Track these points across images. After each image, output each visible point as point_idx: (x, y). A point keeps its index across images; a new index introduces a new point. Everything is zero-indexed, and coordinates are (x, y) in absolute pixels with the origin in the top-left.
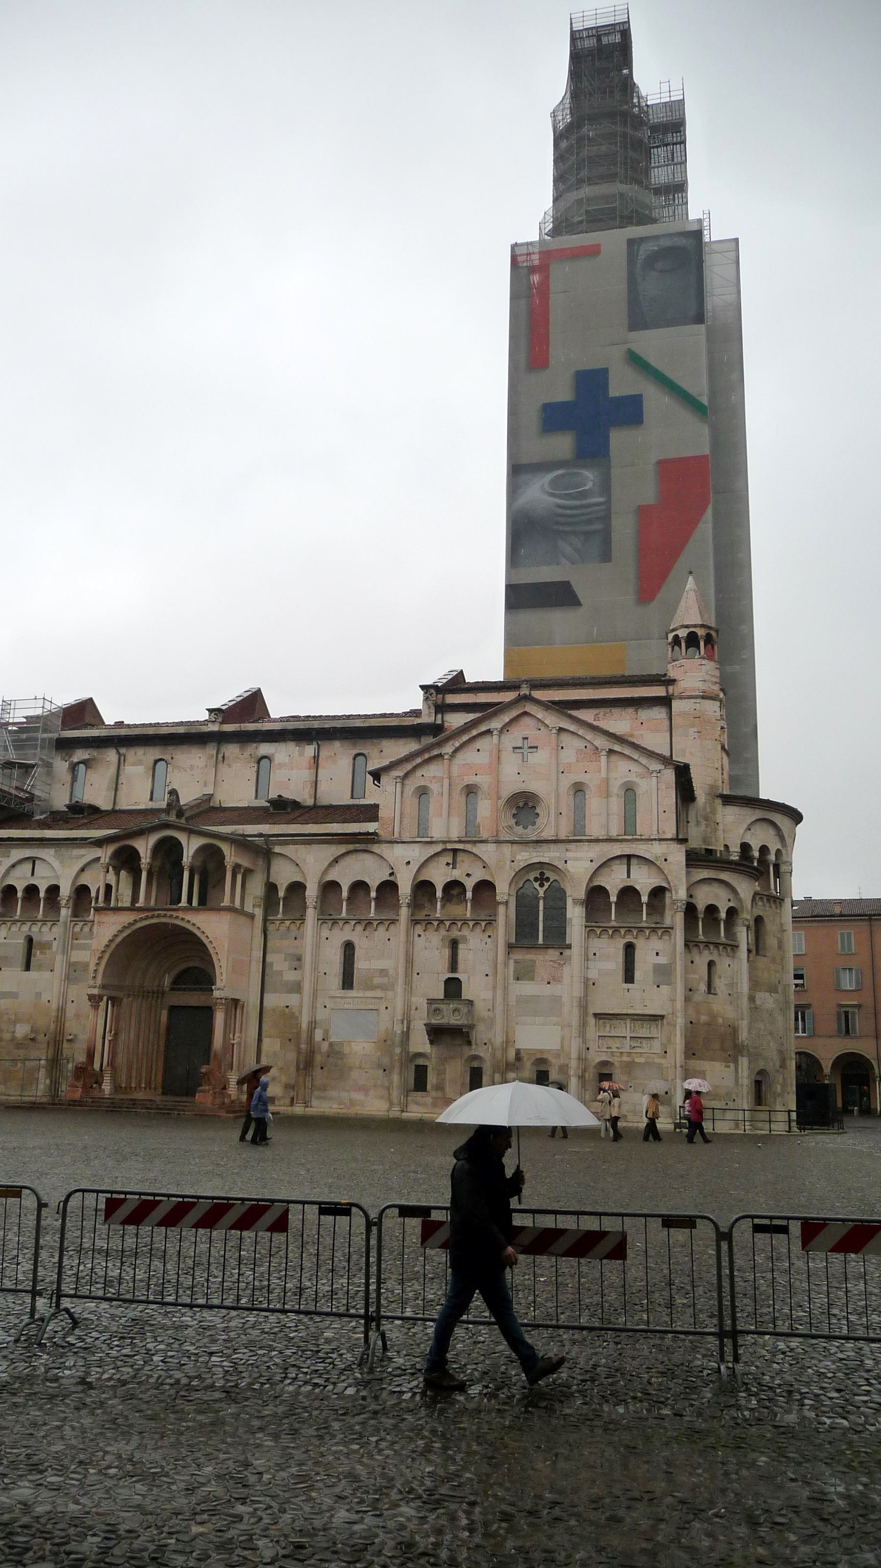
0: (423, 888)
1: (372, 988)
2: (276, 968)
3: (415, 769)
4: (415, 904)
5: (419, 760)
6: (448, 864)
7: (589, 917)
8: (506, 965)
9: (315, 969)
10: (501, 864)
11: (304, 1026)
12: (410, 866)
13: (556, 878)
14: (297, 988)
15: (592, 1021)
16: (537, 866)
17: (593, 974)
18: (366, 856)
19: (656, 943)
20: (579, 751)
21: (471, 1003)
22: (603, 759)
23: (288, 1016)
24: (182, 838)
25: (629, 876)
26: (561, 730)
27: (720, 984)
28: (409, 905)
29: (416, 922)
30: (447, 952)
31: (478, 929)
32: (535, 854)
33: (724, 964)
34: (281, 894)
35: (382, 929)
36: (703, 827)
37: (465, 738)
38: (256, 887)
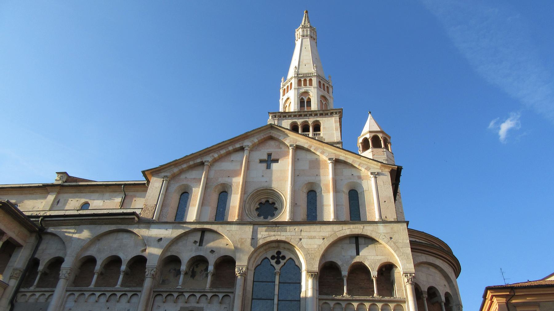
0: (171, 262)
3: (182, 172)
5: (184, 166)
6: (195, 242)
12: (161, 242)
16: (274, 245)
18: (125, 235)
25: (358, 254)
26: (298, 148)
28: (153, 277)
29: (159, 294)
31: (215, 299)
32: (272, 233)
34: (41, 268)
35: (124, 300)
37: (223, 152)
38: (19, 260)
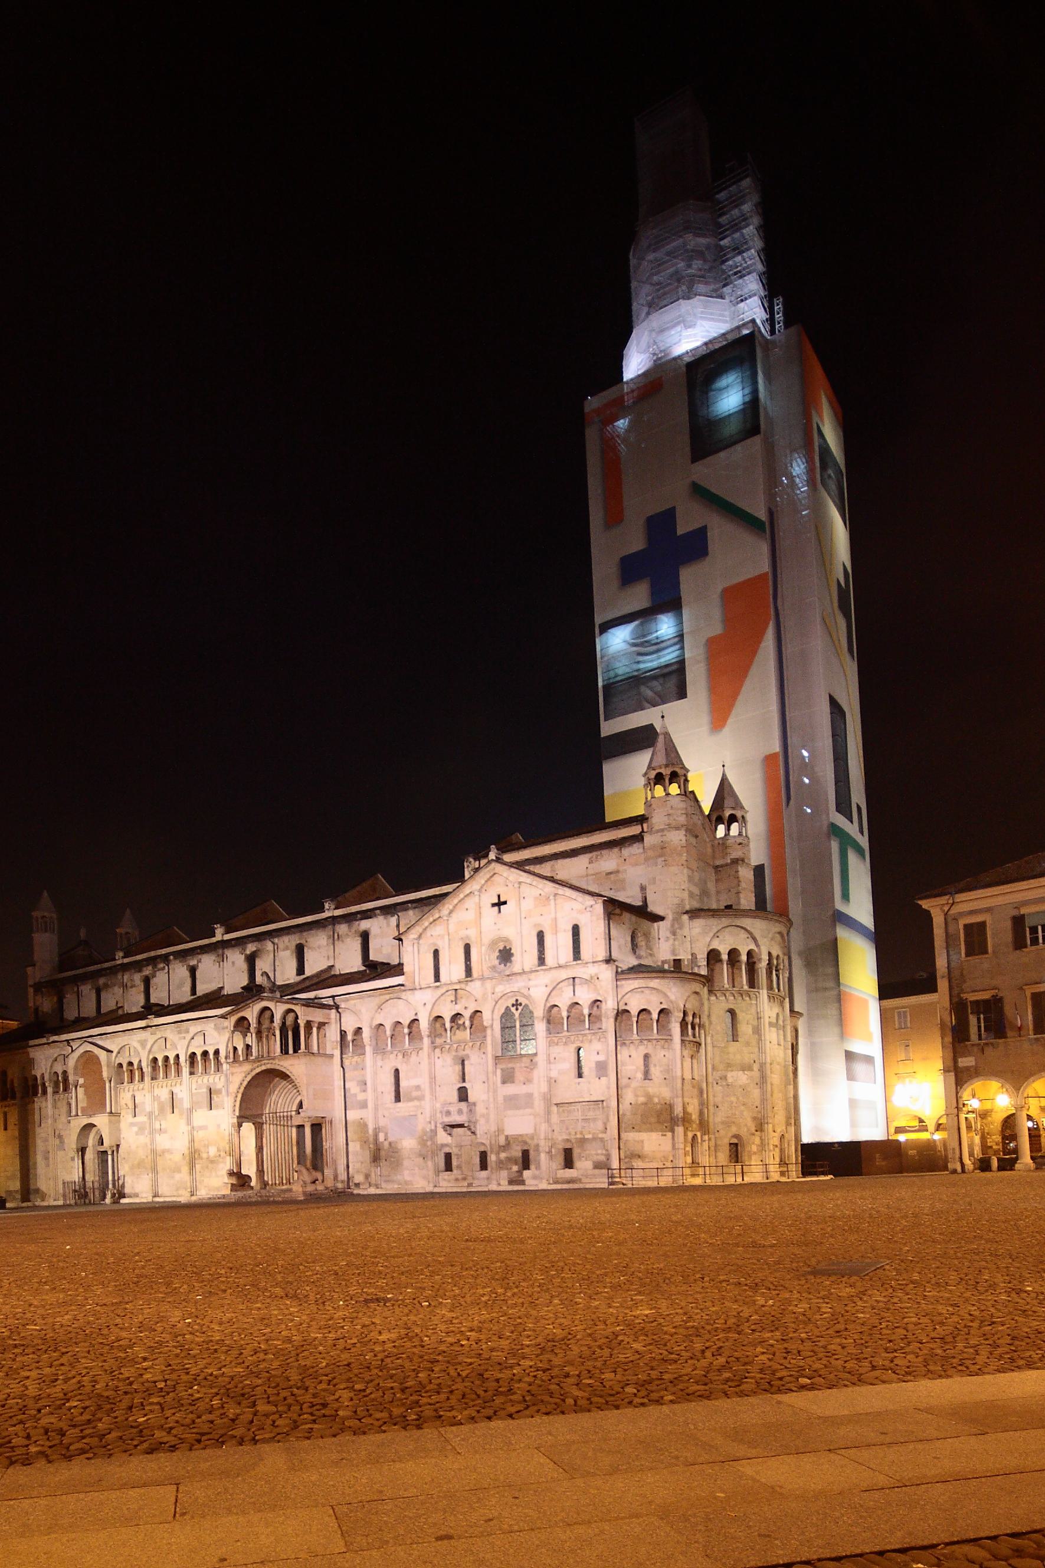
1: (411, 1099)
2: (353, 1091)
4: (434, 1034)
7: (549, 1031)
8: (495, 1073)
9: (375, 1090)
10: (487, 997)
11: (371, 1132)
13: (527, 1002)
14: (364, 1105)
15: (555, 1109)
17: (554, 1074)
19: (597, 1046)
20: (536, 898)
21: (474, 1104)
22: (552, 902)
23: (363, 1125)
24: (270, 1004)
27: (655, 1072)
29: (435, 1048)
30: (459, 1067)
33: (659, 1055)
34: (350, 1037)
36: (671, 941)
